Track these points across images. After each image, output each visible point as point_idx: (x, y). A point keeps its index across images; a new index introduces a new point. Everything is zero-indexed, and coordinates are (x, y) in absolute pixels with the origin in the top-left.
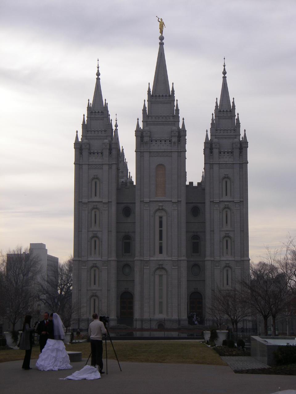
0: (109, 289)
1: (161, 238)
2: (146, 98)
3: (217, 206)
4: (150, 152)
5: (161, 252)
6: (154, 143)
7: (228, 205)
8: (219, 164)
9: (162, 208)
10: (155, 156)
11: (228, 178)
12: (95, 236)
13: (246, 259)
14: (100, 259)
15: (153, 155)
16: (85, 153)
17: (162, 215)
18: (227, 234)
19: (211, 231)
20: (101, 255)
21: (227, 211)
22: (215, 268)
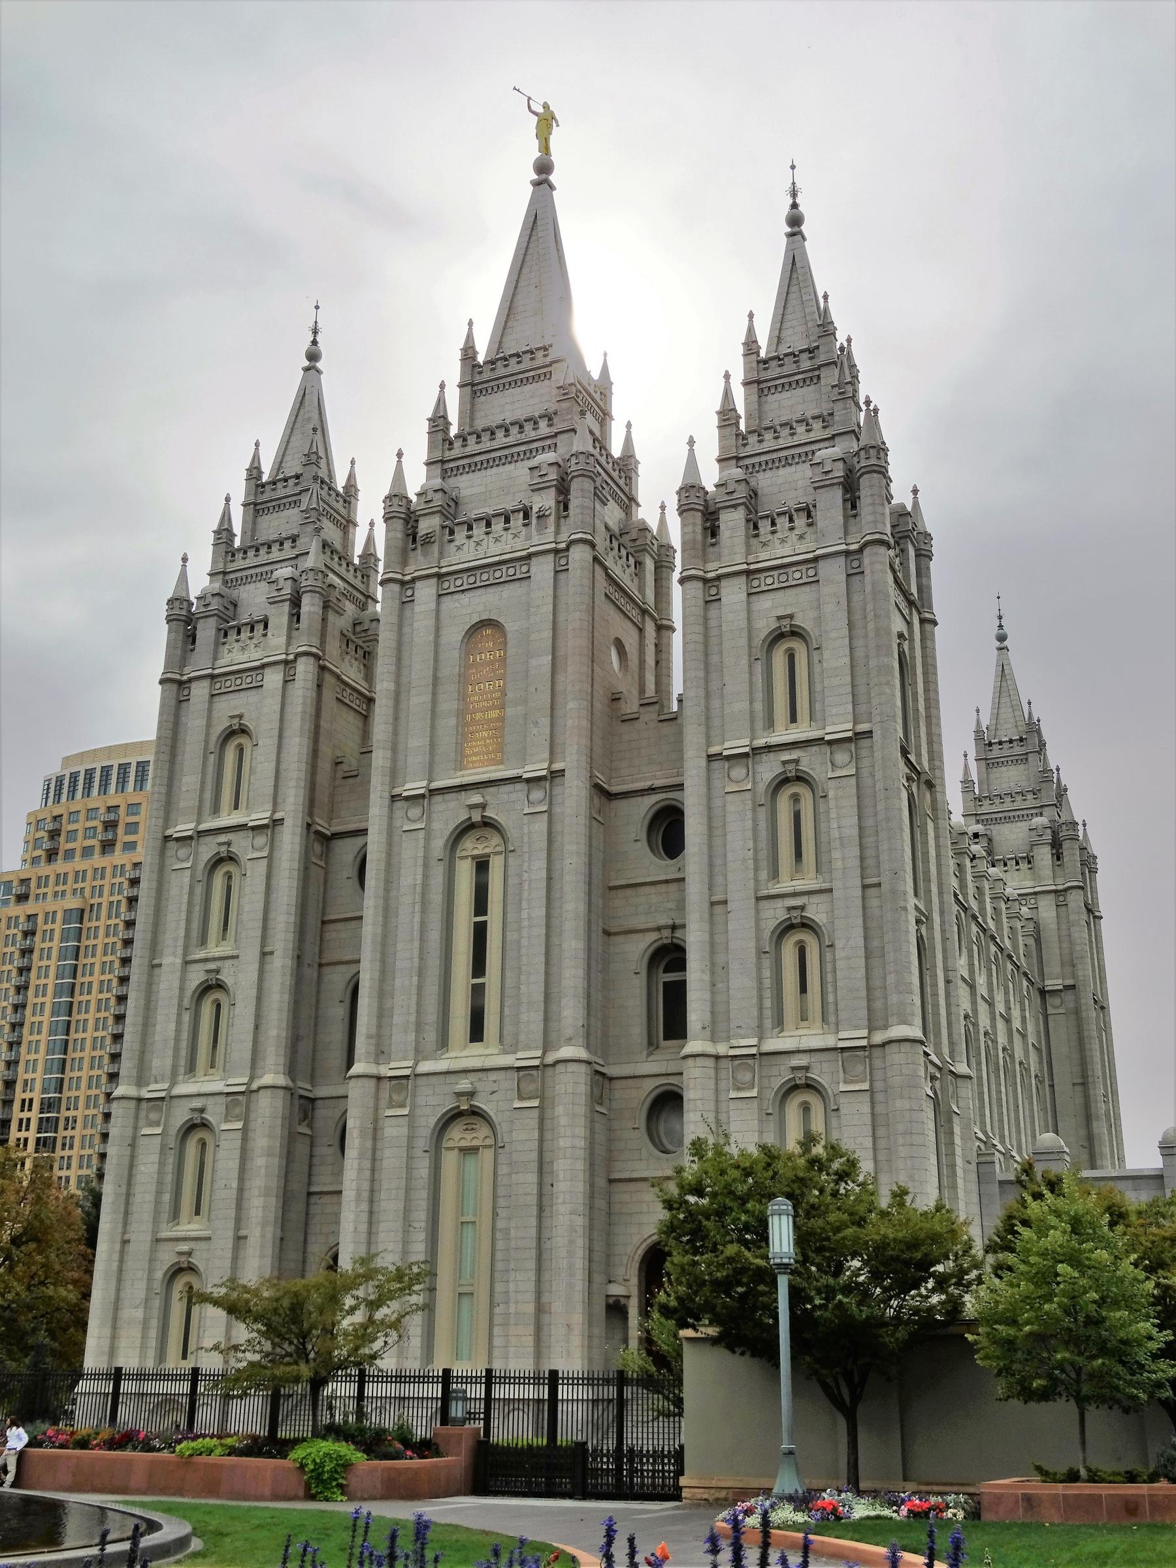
0: (242, 1233)
1: (479, 966)
2: (453, 373)
3: (738, 772)
4: (439, 576)
5: (477, 1033)
6: (460, 535)
7: (797, 761)
8: (748, 573)
9: (483, 817)
10: (463, 591)
11: (796, 633)
12: (212, 986)
14: (219, 1086)
15: (452, 589)
16: (206, 631)
17: (487, 851)
18: (794, 908)
19: (713, 904)
21: (796, 798)
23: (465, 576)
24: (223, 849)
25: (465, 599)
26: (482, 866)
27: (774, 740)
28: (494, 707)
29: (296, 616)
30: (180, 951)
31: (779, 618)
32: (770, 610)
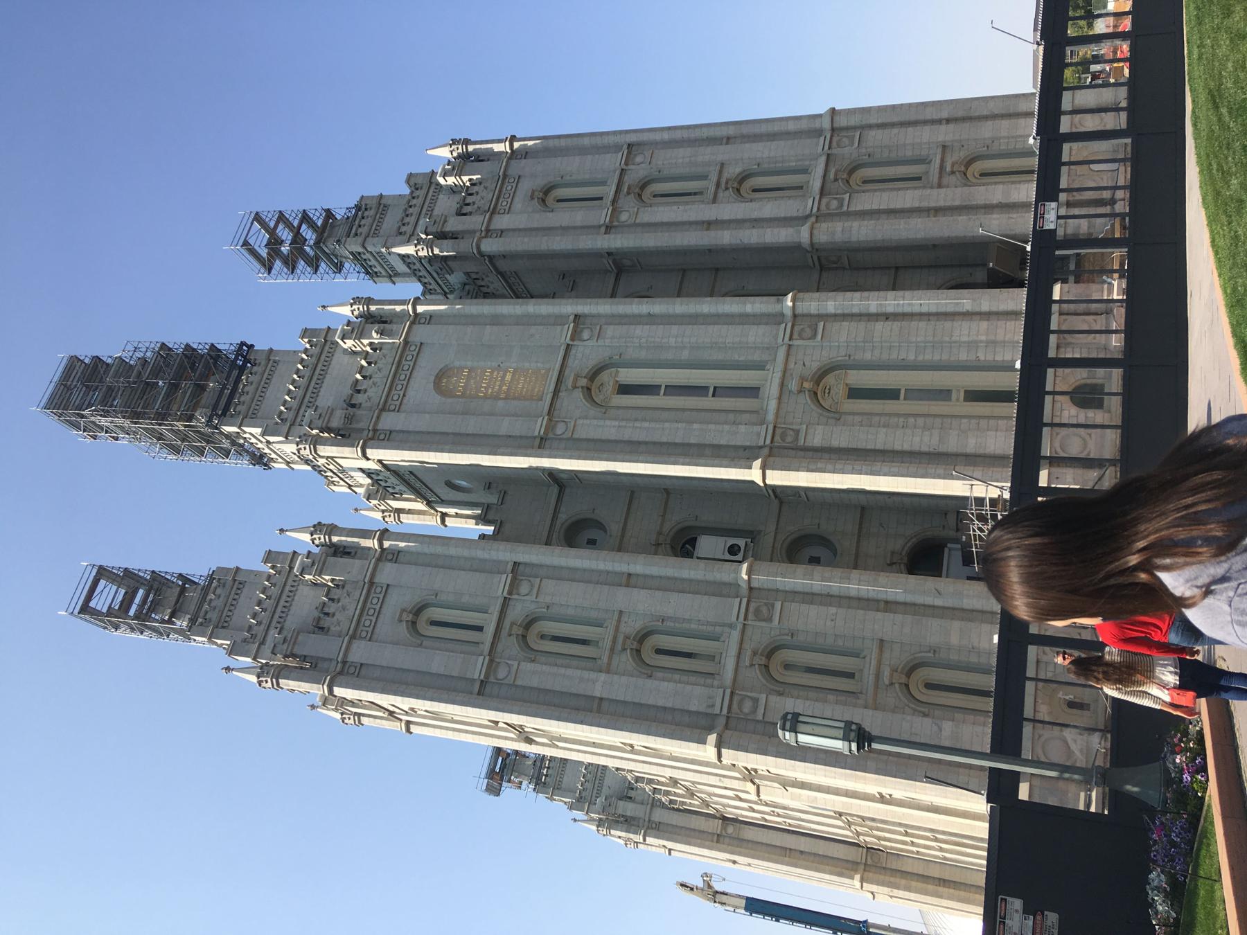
8: (492, 213)
13: (826, 124)
14: (736, 635)
20: (718, 629)
22: (845, 208)
23: (393, 392)
24: (515, 630)
25: (410, 393)
27: (611, 197)
28: (504, 376)
30: (593, 675)
31: (532, 198)
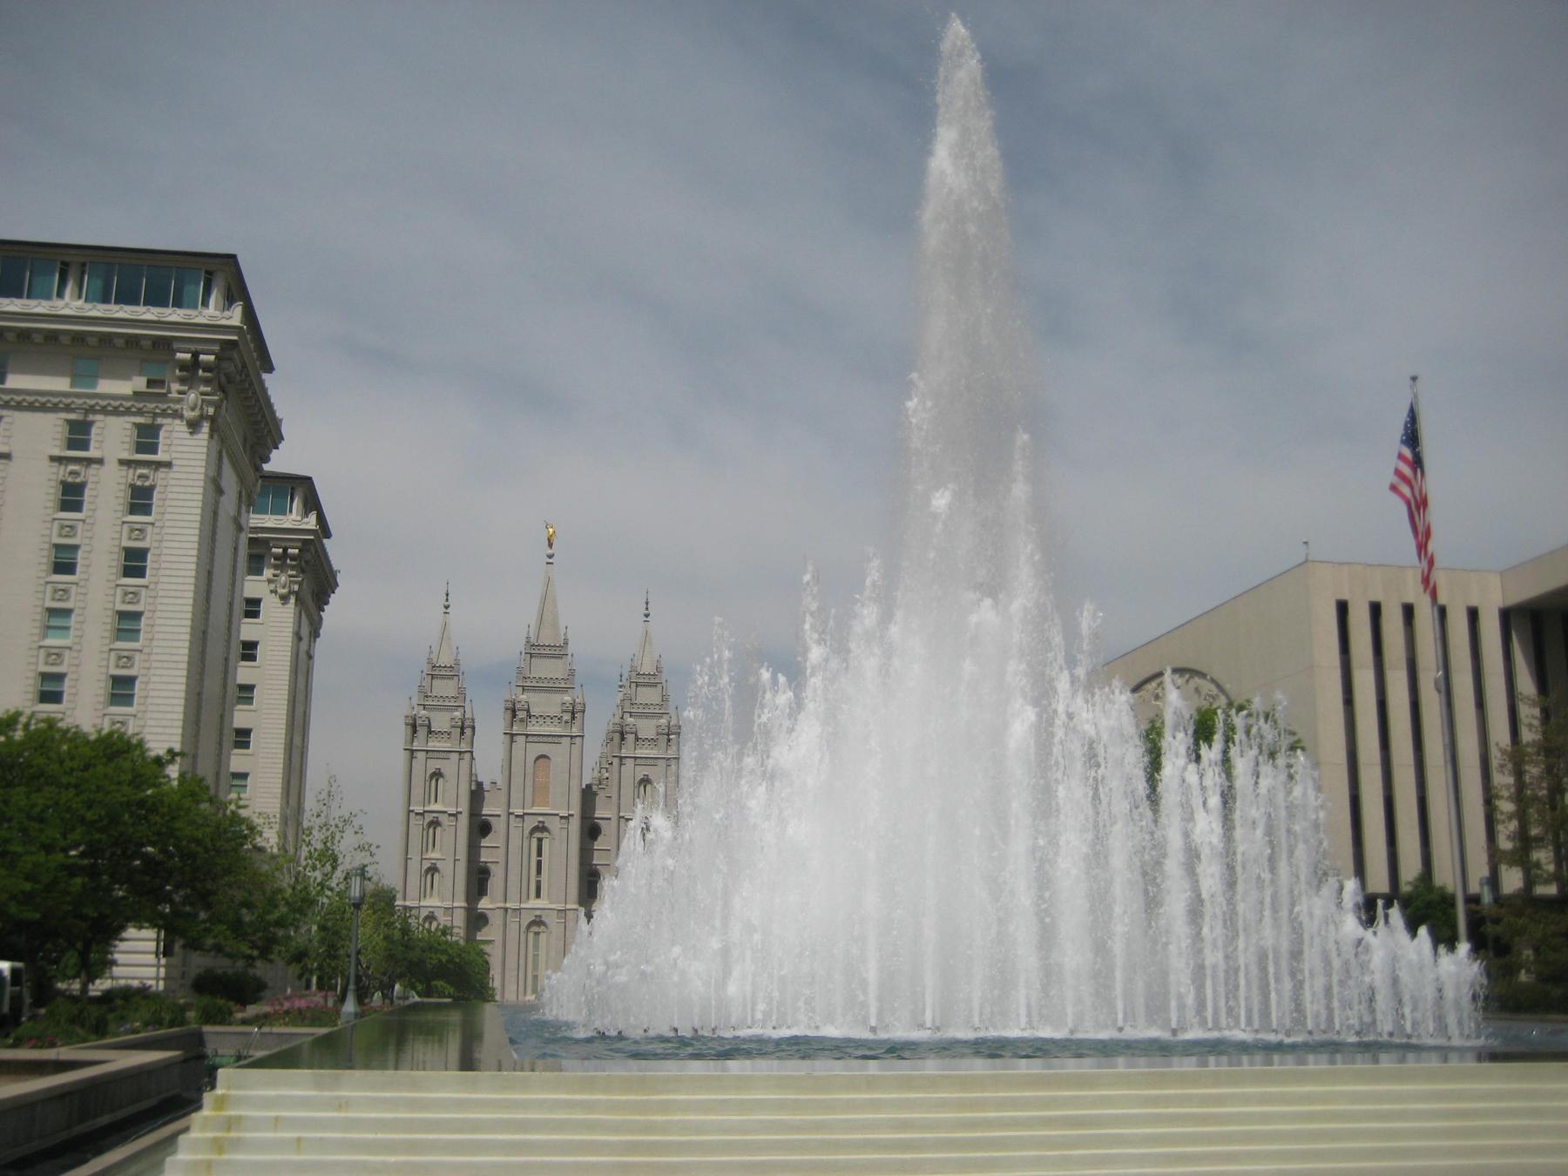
1: (539, 871)
5: (538, 895)
6: (533, 720)
12: (433, 870)
16: (422, 732)
26: (540, 840)
29: (462, 733)
32: (642, 772)
